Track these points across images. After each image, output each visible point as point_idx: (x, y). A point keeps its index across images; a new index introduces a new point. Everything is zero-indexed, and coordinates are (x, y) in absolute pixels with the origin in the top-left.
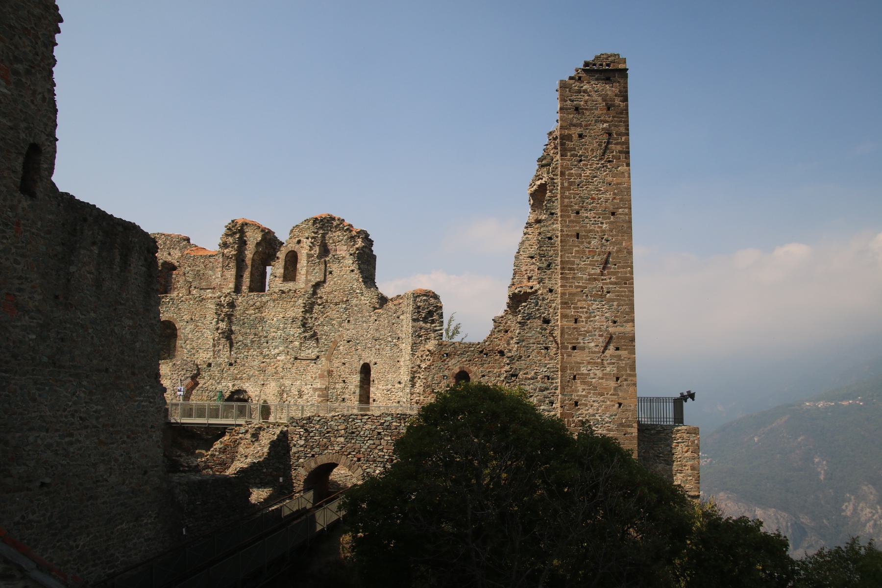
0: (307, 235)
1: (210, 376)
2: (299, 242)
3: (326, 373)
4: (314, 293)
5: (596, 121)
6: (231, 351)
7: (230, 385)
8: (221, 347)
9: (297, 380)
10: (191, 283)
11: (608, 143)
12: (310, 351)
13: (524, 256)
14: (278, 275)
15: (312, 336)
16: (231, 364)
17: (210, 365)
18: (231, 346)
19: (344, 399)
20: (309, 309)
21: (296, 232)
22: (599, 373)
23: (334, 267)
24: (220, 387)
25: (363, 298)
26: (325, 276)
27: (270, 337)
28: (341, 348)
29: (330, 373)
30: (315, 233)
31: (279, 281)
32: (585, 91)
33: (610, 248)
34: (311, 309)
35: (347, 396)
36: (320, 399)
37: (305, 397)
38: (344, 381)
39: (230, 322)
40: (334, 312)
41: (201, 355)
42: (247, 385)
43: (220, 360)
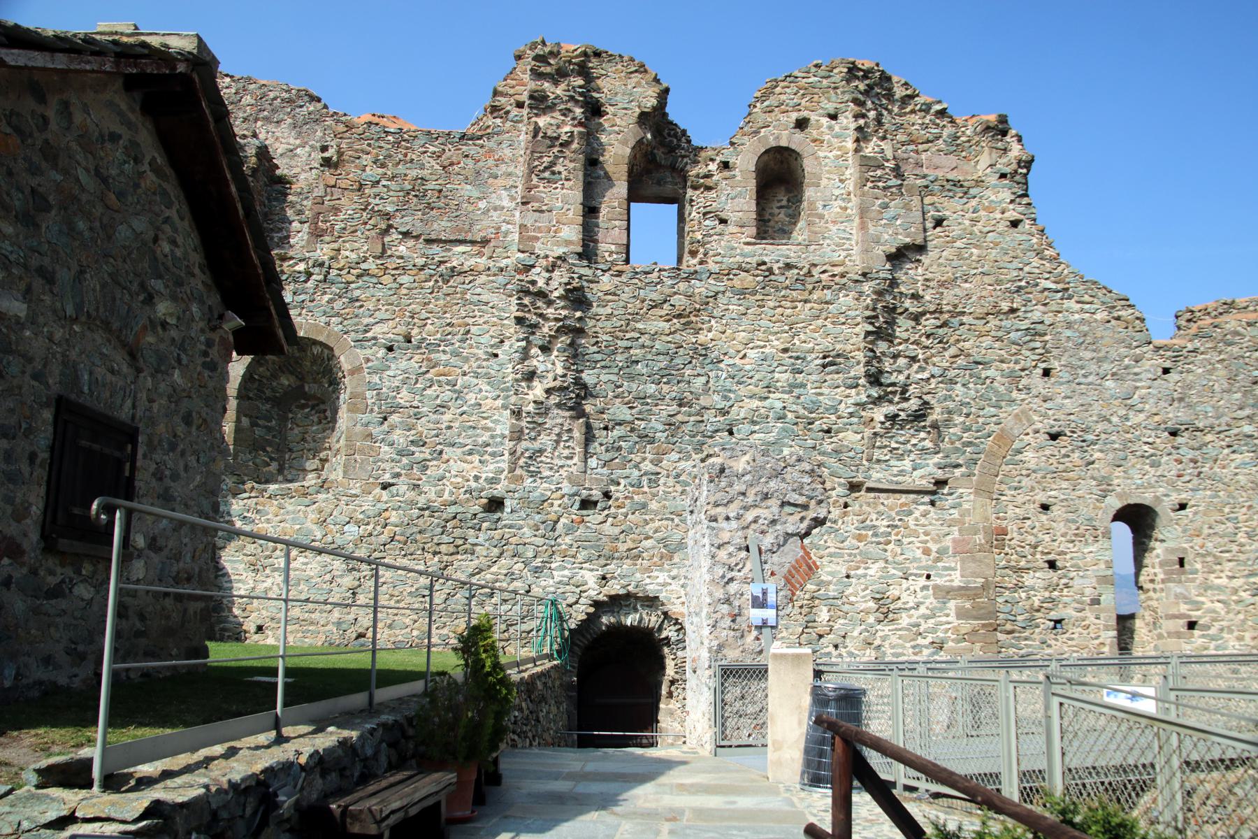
0: (830, 107)
1: (503, 543)
3: (980, 538)
4: (894, 283)
6: (586, 455)
7: (590, 578)
8: (545, 440)
9: (866, 559)
10: (388, 216)
12: (907, 464)
14: (732, 217)
15: (918, 416)
16: (587, 504)
17: (495, 504)
18: (589, 437)
21: (786, 95)
24: (545, 586)
25: (1072, 305)
26: (925, 230)
27: (738, 413)
28: (1029, 455)
30: (856, 101)
34: (891, 323)
35: (1068, 613)
36: (967, 626)
37: (905, 620)
38: (1052, 565)
39: (575, 355)
40: (987, 341)
41: (455, 466)
42: (662, 577)
43: (543, 488)
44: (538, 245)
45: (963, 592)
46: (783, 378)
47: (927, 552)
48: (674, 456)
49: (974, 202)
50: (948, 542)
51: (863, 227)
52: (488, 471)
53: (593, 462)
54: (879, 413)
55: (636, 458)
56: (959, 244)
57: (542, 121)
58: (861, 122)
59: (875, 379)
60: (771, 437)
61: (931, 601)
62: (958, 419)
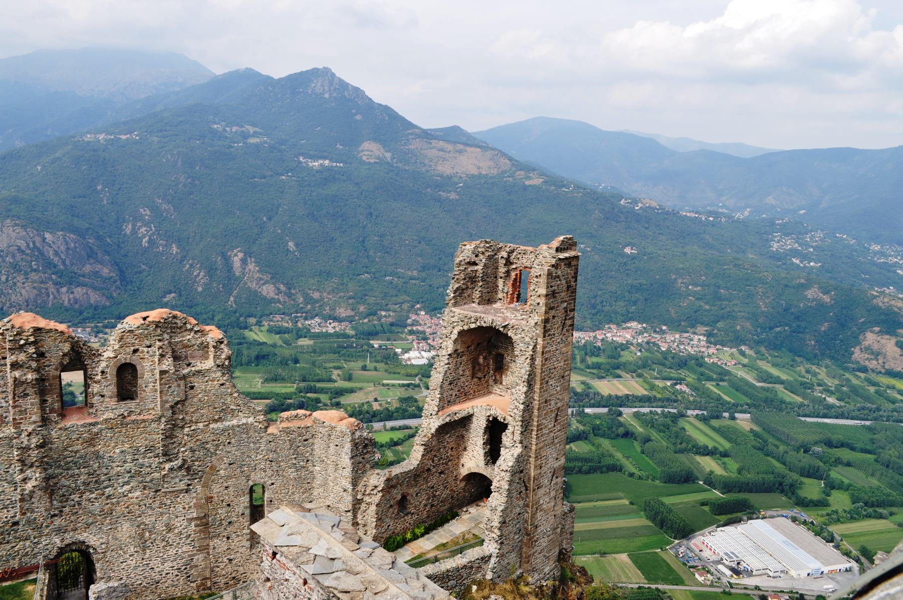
2: (135, 351)
3: (203, 501)
5: (562, 302)
9: (162, 514)
11: (565, 319)
12: (177, 480)
13: (447, 383)
15: (180, 468)
19: (230, 523)
20: (169, 436)
22: (547, 500)
23: (197, 382)
28: (222, 472)
29: (209, 499)
30: (159, 340)
31: (113, 403)
32: (558, 277)
33: (559, 405)
37: (176, 531)
42: (86, 535)
44: (22, 425)
45: (196, 519)
46: (129, 458)
47: (184, 508)
48: (88, 494)
49: (207, 379)
50: (192, 504)
51: (161, 397)
52: (11, 513)
53: (55, 502)
54: (167, 466)
55: (72, 497)
56: (200, 396)
57: (17, 374)
58: (161, 351)
59: (165, 455)
60: (126, 480)
61: (186, 524)
62: (197, 463)
